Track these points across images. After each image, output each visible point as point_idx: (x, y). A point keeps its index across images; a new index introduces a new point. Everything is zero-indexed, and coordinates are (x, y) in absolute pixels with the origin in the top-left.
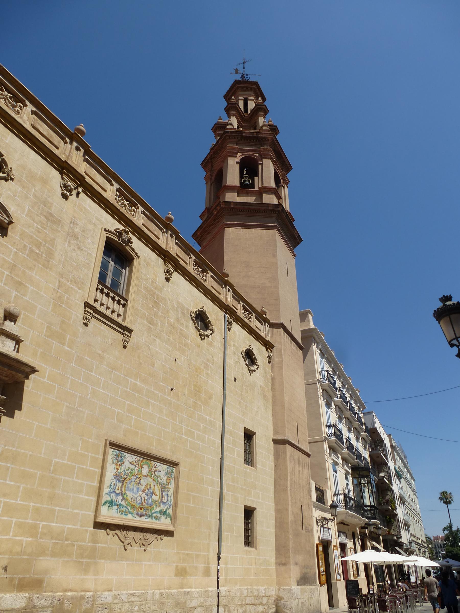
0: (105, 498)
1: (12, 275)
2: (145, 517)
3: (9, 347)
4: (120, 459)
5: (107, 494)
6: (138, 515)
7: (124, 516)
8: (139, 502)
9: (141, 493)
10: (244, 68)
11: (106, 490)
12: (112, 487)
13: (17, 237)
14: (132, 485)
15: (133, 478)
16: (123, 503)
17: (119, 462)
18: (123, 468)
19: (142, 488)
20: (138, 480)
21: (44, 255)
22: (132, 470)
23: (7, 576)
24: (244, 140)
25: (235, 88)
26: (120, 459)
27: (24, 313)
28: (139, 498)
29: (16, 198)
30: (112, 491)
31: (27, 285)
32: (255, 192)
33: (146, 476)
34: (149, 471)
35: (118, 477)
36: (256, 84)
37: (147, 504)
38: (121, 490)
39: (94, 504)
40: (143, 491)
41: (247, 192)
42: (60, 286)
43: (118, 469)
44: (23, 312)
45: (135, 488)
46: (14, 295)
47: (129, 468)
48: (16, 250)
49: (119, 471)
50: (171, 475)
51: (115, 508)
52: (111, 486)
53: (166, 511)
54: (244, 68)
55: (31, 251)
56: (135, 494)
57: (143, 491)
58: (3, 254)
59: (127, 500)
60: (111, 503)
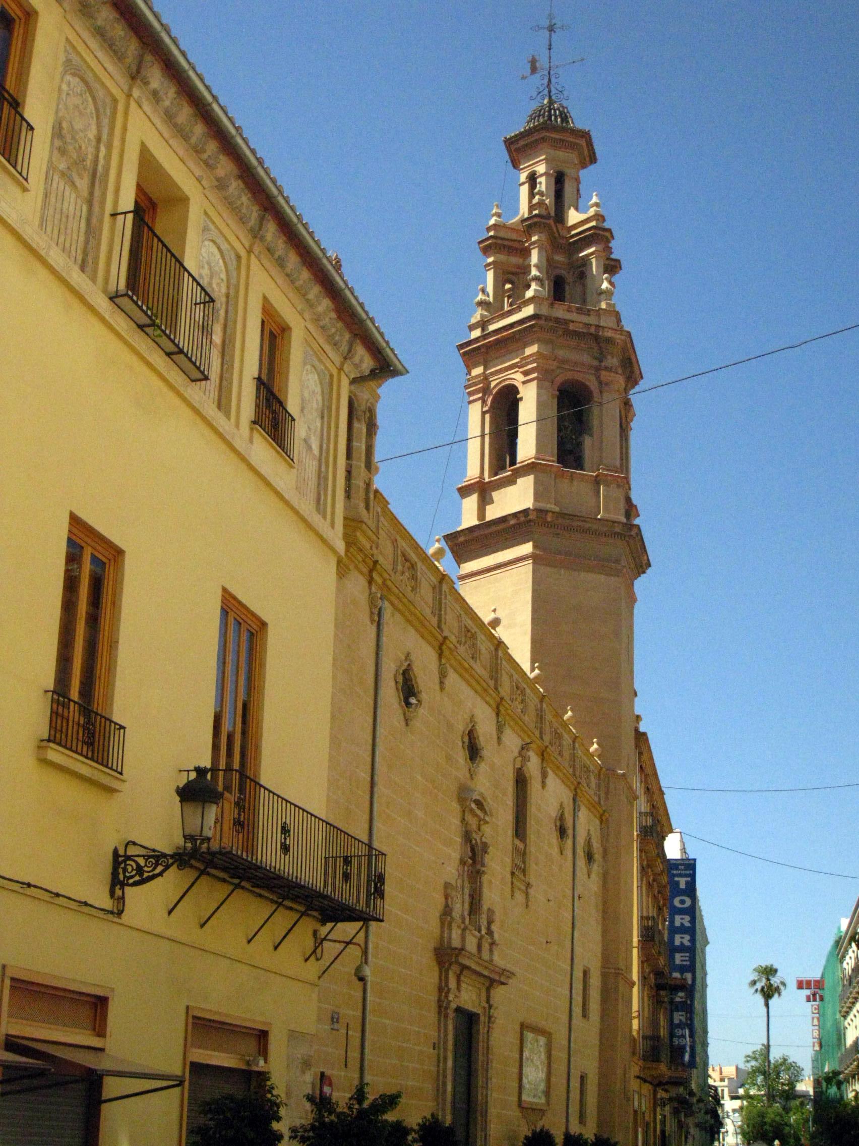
10: (550, 49)
25: (536, 136)
32: (587, 477)
36: (586, 136)
41: (571, 476)
54: (550, 49)
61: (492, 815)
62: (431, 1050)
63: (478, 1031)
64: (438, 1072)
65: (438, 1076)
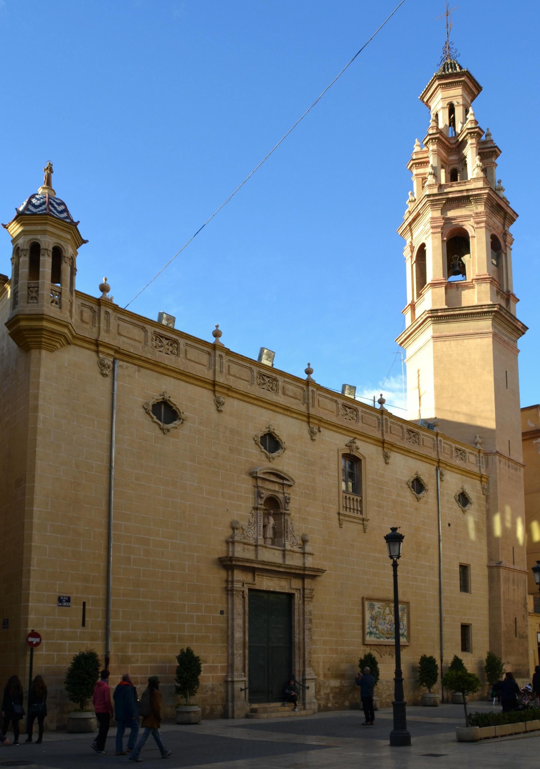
0: (367, 631)
2: (390, 639)
4: (372, 607)
5: (368, 628)
6: (386, 638)
7: (378, 640)
8: (386, 630)
9: (387, 625)
11: (367, 626)
12: (370, 624)
14: (381, 621)
15: (381, 617)
16: (377, 632)
17: (372, 607)
18: (374, 612)
19: (387, 622)
20: (384, 617)
21: (312, 493)
22: (380, 612)
24: (451, 203)
26: (372, 607)
28: (386, 628)
29: (291, 461)
30: (370, 626)
33: (388, 614)
34: (390, 611)
35: (373, 618)
37: (391, 631)
38: (375, 625)
39: (361, 635)
40: (388, 624)
43: (371, 613)
45: (383, 622)
47: (378, 611)
49: (373, 614)
50: (404, 610)
51: (373, 635)
52: (369, 623)
53: (403, 633)
55: (305, 493)
56: (383, 626)
57: (388, 624)
59: (379, 630)
60: (371, 633)
61: (293, 480)
62: (219, 615)
63: (295, 603)
64: (228, 627)
65: (228, 629)
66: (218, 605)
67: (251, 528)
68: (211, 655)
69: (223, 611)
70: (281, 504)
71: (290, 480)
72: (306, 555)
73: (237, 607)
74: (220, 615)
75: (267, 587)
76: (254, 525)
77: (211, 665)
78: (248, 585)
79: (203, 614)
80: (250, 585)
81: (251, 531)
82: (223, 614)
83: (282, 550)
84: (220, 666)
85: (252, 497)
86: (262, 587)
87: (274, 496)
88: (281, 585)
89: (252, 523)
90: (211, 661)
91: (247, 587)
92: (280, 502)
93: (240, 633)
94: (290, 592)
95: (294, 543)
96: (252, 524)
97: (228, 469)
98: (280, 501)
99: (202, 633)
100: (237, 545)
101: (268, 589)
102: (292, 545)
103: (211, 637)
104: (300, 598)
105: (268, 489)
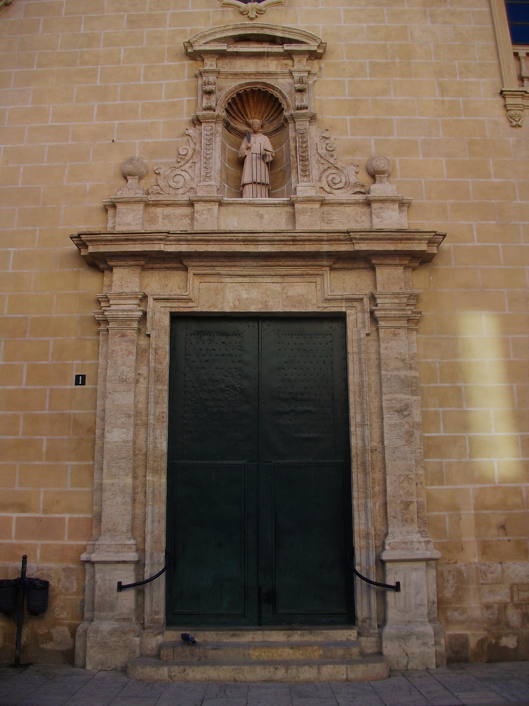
1: (358, 117)
3: (391, 218)
13: (345, 60)
21: (398, 61)
23: (510, 538)
27: (400, 160)
31: (388, 117)
42: (444, 91)
44: (397, 159)
46: (373, 143)
48: (350, 79)
58: (333, 94)
66: (70, 362)
67: (183, 168)
68: (42, 490)
69: (84, 377)
70: (285, 98)
71: (305, 40)
72: (374, 205)
73: (119, 362)
74: (74, 387)
75: (237, 303)
76: (192, 157)
77: (40, 515)
78: (169, 304)
79: (23, 387)
80: (175, 305)
81: (183, 173)
82: (83, 383)
83: (284, 205)
84: (70, 519)
85: (189, 101)
86: (220, 306)
87: (259, 86)
88: (290, 294)
89: (186, 155)
90: (41, 507)
91: (168, 310)
92: (279, 96)
93: (125, 430)
94: (326, 310)
95: (335, 184)
96: (187, 158)
97: (122, 59)
98: (280, 92)
99: (17, 433)
100: (125, 211)
101: (241, 309)
102: (328, 189)
103: (45, 445)
104: (364, 323)
105: (236, 74)
